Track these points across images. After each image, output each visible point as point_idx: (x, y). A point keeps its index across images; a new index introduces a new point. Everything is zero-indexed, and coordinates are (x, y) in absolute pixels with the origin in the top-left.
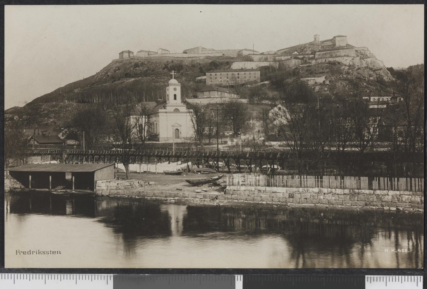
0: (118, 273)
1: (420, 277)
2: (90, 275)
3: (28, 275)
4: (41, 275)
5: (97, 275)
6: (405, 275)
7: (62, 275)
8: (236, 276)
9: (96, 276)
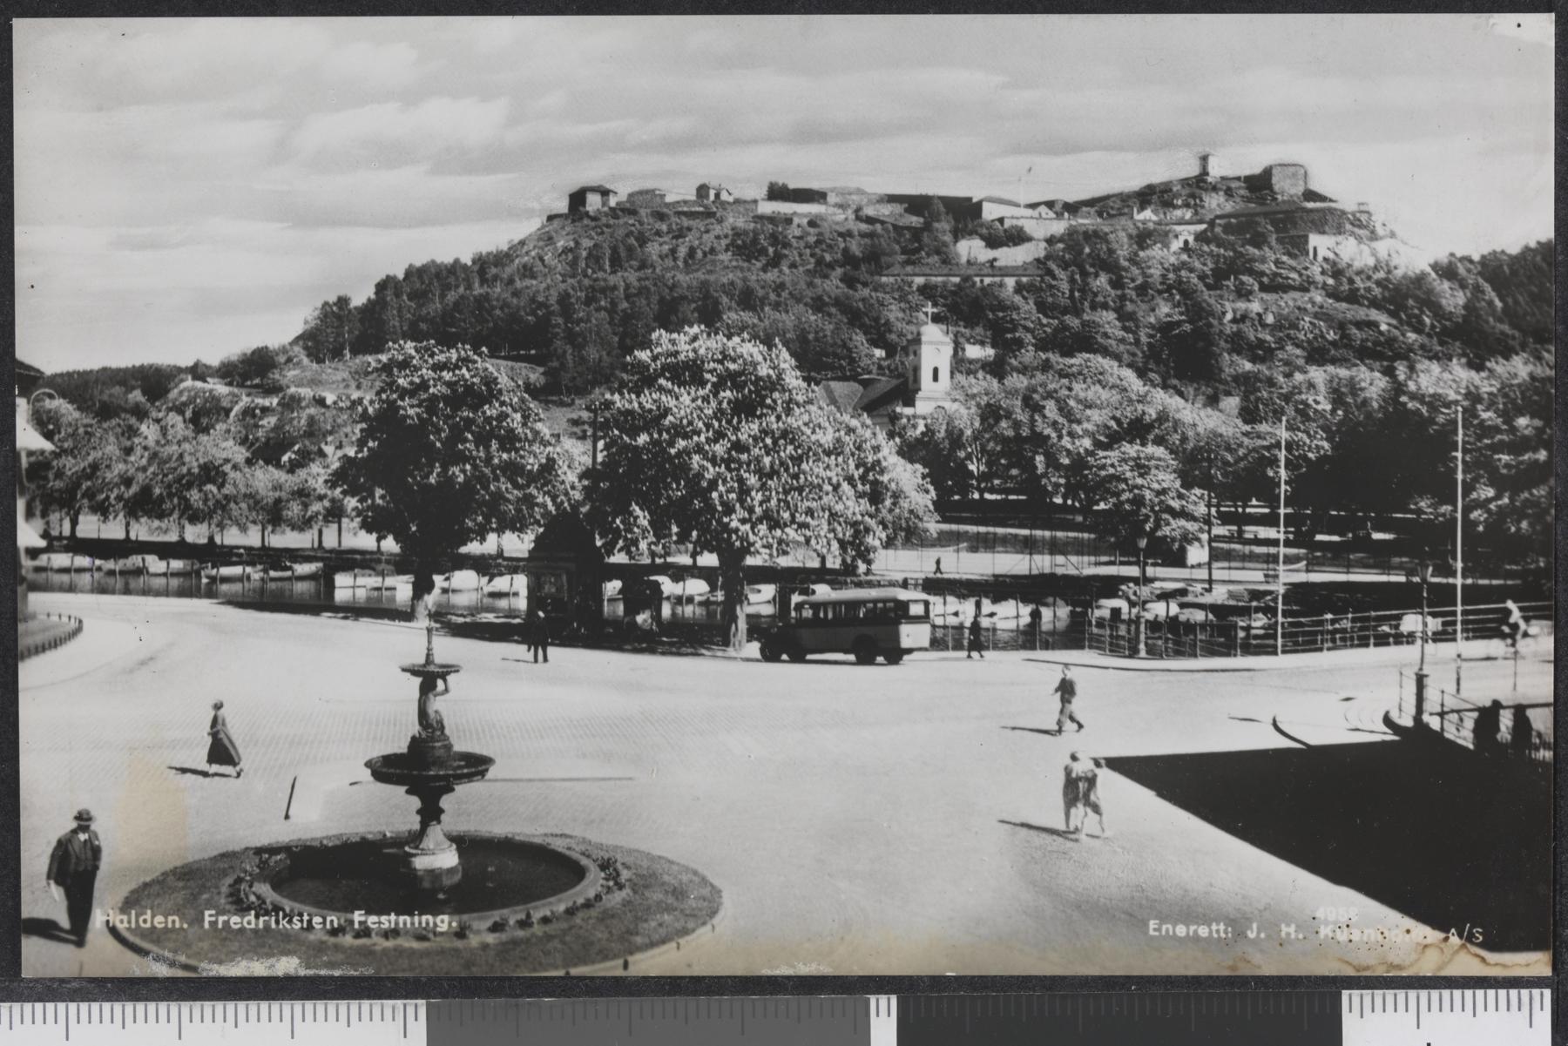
0: (444, 996)
1: (1542, 994)
2: (343, 1004)
3: (118, 1006)
4: (163, 1006)
5: (366, 1004)
6: (1486, 988)
7: (241, 1005)
8: (873, 999)
9: (408, 1008)
